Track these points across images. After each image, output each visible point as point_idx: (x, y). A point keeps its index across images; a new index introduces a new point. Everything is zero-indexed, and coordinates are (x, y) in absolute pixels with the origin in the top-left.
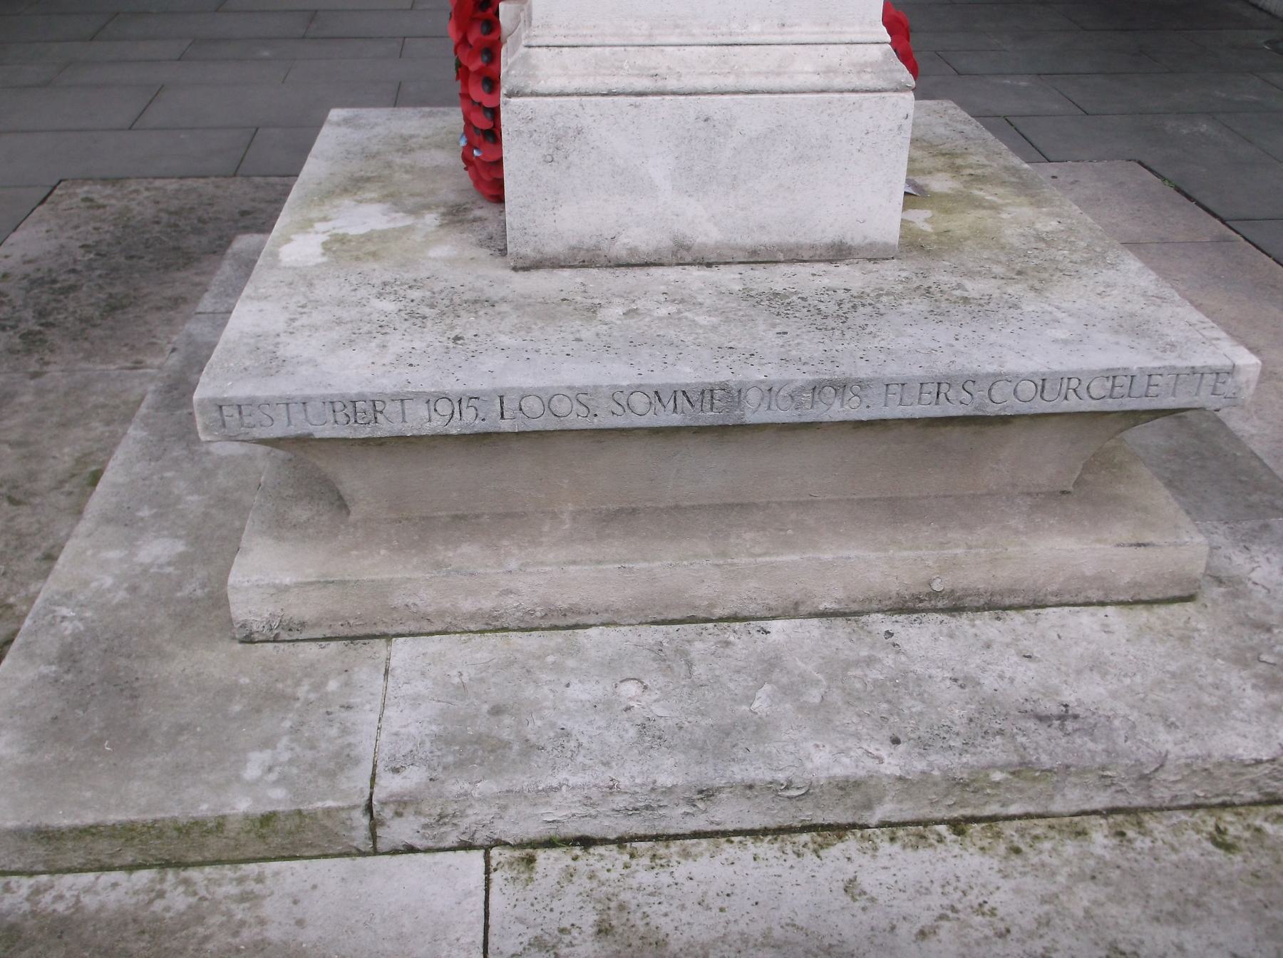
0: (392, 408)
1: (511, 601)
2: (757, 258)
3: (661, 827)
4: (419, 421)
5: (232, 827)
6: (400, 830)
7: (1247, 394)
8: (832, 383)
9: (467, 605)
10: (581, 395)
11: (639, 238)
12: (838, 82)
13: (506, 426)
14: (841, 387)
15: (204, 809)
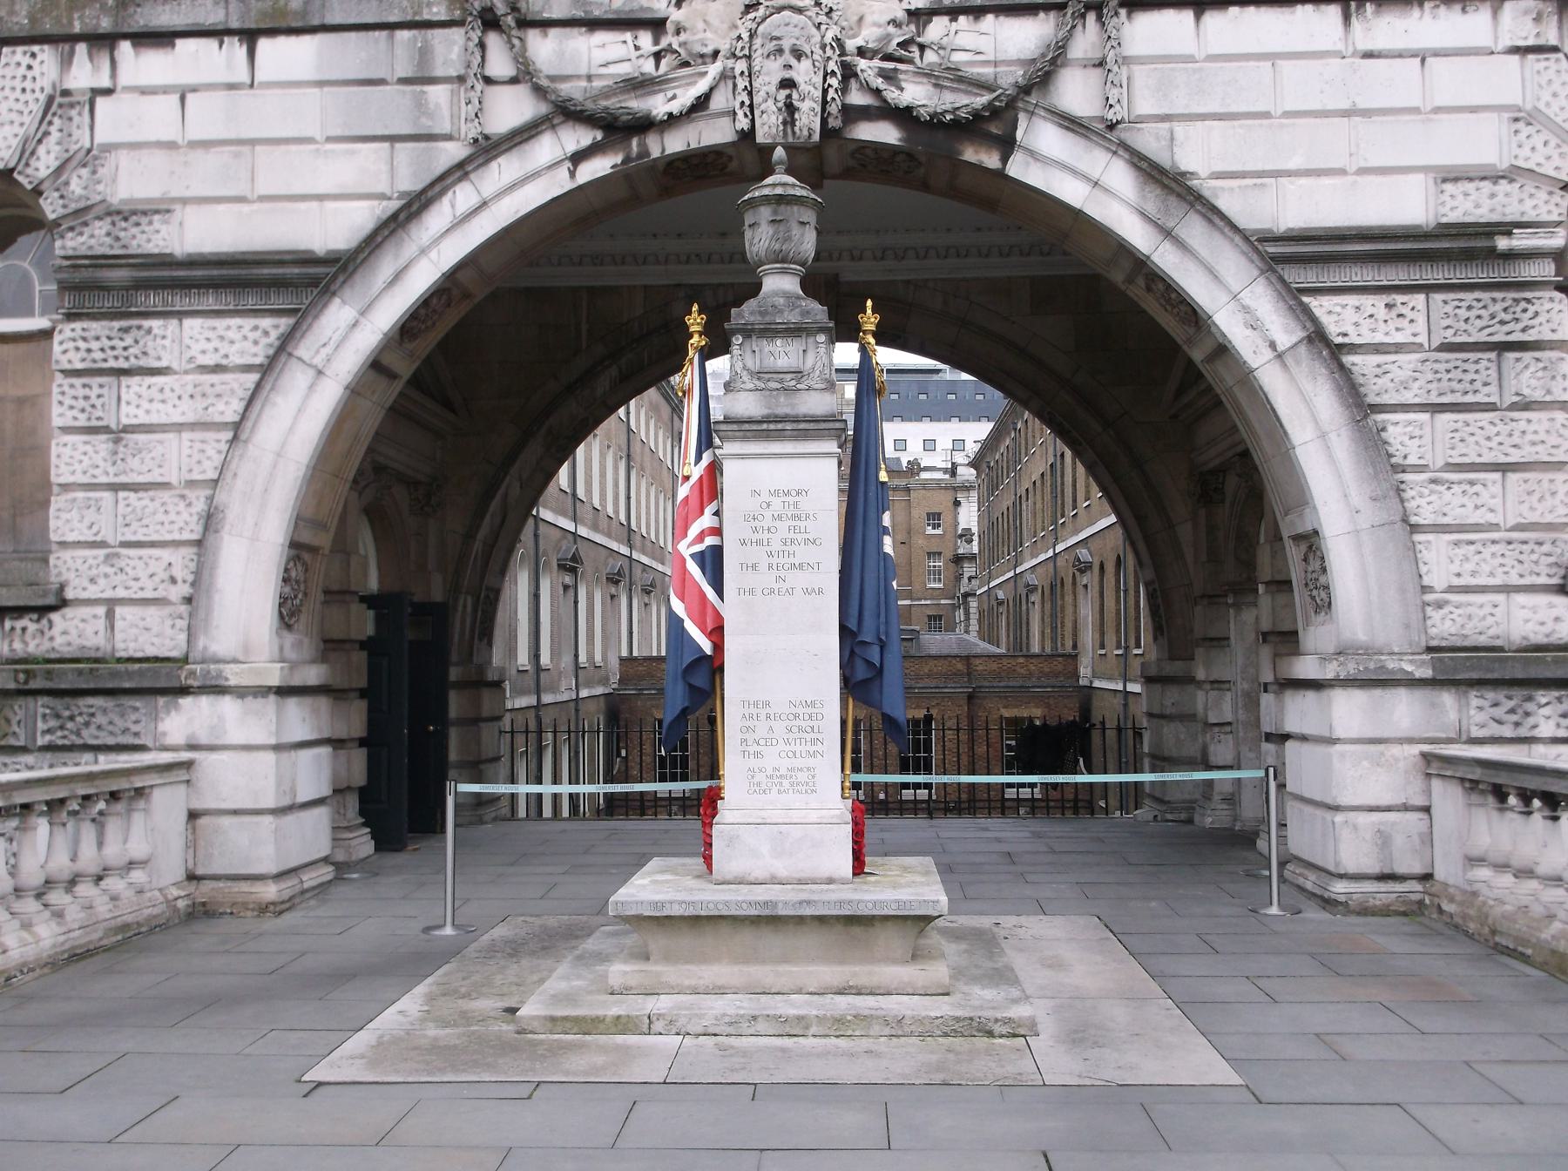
2: (800, 882)
4: (676, 911)
7: (945, 911)
9: (687, 982)
10: (726, 903)
11: (759, 874)
14: (808, 902)
15: (600, 1013)
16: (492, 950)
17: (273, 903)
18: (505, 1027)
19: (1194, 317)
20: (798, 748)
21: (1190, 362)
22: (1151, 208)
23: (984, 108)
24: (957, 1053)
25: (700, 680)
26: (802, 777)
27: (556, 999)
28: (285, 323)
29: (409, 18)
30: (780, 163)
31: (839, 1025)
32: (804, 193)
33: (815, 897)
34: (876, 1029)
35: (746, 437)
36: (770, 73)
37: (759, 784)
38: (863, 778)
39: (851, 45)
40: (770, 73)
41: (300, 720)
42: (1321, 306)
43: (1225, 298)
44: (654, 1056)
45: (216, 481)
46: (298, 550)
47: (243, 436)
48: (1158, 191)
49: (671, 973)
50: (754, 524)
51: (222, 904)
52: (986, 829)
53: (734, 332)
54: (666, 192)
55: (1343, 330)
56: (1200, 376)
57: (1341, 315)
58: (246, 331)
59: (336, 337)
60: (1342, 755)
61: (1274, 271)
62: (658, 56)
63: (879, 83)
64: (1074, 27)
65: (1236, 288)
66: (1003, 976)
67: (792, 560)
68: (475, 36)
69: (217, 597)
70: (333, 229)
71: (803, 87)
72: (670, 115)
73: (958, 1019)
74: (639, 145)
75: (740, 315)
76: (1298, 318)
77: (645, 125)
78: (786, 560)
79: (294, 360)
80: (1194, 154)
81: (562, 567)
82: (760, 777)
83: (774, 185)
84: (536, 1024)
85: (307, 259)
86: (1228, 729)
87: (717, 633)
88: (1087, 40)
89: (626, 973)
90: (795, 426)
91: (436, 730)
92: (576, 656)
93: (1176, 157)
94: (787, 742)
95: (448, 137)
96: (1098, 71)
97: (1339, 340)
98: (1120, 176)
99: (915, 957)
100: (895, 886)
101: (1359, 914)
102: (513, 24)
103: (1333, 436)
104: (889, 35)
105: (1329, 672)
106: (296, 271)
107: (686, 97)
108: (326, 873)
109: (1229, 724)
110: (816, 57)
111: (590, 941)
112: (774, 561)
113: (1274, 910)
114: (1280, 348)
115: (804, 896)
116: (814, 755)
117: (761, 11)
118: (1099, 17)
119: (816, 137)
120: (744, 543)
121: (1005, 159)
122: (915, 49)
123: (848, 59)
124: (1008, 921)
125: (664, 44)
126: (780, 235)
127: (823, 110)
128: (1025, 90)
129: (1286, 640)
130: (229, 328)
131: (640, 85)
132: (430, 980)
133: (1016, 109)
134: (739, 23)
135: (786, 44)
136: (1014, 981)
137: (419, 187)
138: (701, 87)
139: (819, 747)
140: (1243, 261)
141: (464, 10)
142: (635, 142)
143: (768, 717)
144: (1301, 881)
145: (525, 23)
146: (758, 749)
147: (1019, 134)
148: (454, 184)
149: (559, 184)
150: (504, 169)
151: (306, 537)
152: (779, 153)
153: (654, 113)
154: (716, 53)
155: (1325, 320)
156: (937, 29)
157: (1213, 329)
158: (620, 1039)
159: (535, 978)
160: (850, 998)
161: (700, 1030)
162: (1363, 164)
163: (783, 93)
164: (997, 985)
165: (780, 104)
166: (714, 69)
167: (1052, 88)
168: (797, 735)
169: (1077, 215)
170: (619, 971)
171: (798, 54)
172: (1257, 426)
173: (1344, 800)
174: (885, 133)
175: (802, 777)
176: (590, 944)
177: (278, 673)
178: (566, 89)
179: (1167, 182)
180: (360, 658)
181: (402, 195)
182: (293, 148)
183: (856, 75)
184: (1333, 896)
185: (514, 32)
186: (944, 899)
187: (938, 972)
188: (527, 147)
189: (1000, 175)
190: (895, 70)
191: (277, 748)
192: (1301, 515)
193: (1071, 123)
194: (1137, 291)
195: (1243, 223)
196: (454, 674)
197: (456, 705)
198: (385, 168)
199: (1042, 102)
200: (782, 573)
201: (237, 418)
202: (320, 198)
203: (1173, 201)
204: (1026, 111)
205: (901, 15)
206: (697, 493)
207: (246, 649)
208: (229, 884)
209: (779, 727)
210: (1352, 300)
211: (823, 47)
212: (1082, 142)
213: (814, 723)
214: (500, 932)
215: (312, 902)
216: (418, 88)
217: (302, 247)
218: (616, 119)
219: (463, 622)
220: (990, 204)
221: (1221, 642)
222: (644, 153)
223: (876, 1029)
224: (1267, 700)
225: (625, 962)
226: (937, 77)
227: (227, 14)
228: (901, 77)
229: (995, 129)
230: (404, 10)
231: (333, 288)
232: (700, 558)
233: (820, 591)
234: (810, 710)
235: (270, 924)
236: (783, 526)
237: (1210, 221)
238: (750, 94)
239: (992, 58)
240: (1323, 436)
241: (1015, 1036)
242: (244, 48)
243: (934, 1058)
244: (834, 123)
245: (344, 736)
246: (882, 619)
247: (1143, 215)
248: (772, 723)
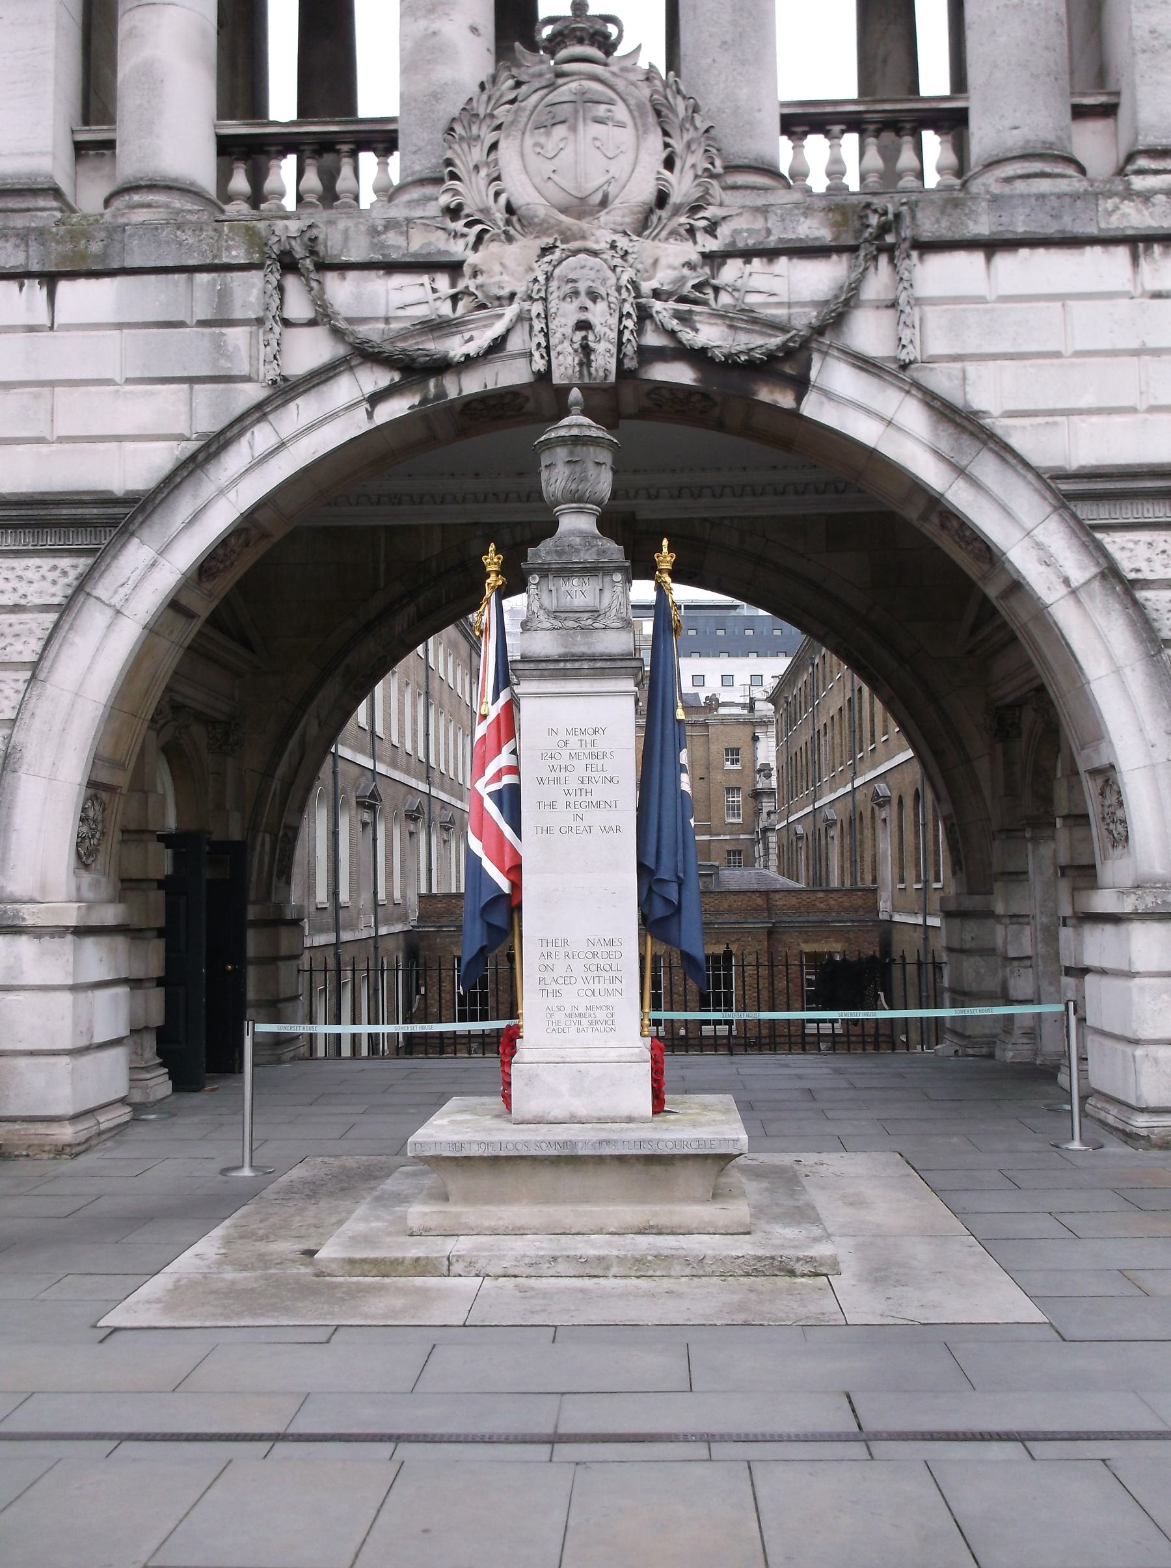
0: (467, 1146)
1: (501, 1223)
2: (600, 1121)
3: (540, 1273)
4: (475, 1151)
5: (407, 1262)
6: (457, 1268)
7: (746, 1149)
8: (604, 1141)
9: (486, 1224)
10: (526, 1144)
11: (557, 1112)
12: (624, 1059)
13: (502, 1154)
14: (608, 1142)
15: (399, 1254)
16: (290, 1191)
17: (69, 1145)
18: (303, 1270)
19: (988, 554)
20: (596, 986)
21: (985, 599)
22: (944, 446)
23: (779, 348)
24: (761, 1293)
25: (498, 919)
26: (601, 1015)
27: (355, 1241)
28: (84, 563)
29: (208, 261)
30: (577, 404)
31: (640, 1265)
32: (600, 434)
33: (615, 1137)
34: (677, 1269)
35: (543, 675)
36: (566, 315)
38: (663, 1015)
39: (646, 287)
40: (566, 315)
41: (97, 962)
42: (1113, 542)
43: (1019, 535)
44: (453, 1298)
45: (14, 721)
46: (95, 789)
47: (42, 676)
48: (951, 430)
49: (470, 1214)
50: (551, 762)
51: (17, 1147)
52: (787, 1066)
53: (531, 571)
54: (462, 432)
55: (1136, 566)
56: (994, 612)
57: (1133, 552)
58: (43, 571)
59: (135, 577)
60: (1142, 989)
61: (1067, 508)
62: (455, 299)
63: (674, 324)
64: (866, 269)
65: (1029, 525)
66: (804, 1214)
67: (589, 798)
68: (274, 279)
69: (14, 837)
70: (131, 470)
71: (599, 329)
72: (467, 356)
73: (759, 1259)
74: (436, 386)
75: (536, 555)
76: (1091, 554)
77: (442, 366)
78: (584, 798)
79: (92, 600)
80: (988, 393)
81: (361, 804)
83: (570, 426)
84: (334, 1266)
85: (105, 499)
86: (1028, 963)
87: (515, 871)
88: (879, 281)
89: (425, 1214)
90: (591, 664)
91: (234, 969)
92: (375, 893)
93: (969, 397)
95: (247, 379)
96: (891, 312)
97: (1132, 576)
98: (913, 415)
99: (716, 1195)
100: (695, 1124)
101: (1160, 1148)
102: (311, 268)
103: (1127, 671)
104: (683, 277)
105: (1128, 905)
106: (95, 511)
107: (483, 338)
108: (122, 1114)
109: (1029, 958)
110: (612, 299)
111: (389, 1181)
112: (572, 799)
113: (1076, 1145)
114: (1074, 584)
115: (603, 1136)
116: (613, 993)
117: (557, 254)
118: (891, 260)
119: (612, 378)
120: (541, 781)
121: (799, 399)
122: (709, 291)
123: (643, 300)
124: (809, 1158)
125: (461, 286)
126: (576, 475)
127: (619, 351)
128: (819, 331)
129: (1084, 874)
130: (27, 568)
131: (437, 327)
132: (227, 1222)
133: (810, 350)
134: (536, 265)
135: (582, 287)
136: (817, 1220)
137: (217, 428)
138: (498, 328)
140: (1036, 498)
141: (263, 253)
142: (432, 383)
143: (567, 956)
144: (1102, 1115)
145: (324, 266)
146: (557, 987)
147: (813, 374)
148: (253, 424)
149: (357, 425)
150: (302, 411)
151: (104, 777)
152: (575, 394)
153: (451, 354)
154: (512, 296)
155: (1118, 556)
156: (731, 271)
157: (1007, 566)
158: (419, 1281)
159: (334, 1220)
160: (650, 1239)
161: (500, 1271)
162: (1153, 402)
163: (579, 335)
164: (799, 1223)
165: (576, 346)
166: (511, 312)
167: (845, 329)
168: (596, 974)
169: (871, 454)
170: (418, 1213)
171: (594, 296)
172: (1050, 658)
173: (1146, 1033)
174: (681, 374)
175: (601, 1015)
176: (389, 1185)
177: (74, 913)
178: (364, 331)
179: (959, 421)
180: (158, 897)
181: (201, 435)
182: (93, 389)
183: (651, 317)
184: (1135, 1130)
185: (312, 276)
186: (744, 1137)
187: (739, 1211)
188: (324, 388)
189: (795, 414)
190: (690, 312)
191: (74, 988)
192: (1097, 750)
193: (865, 364)
194: (931, 529)
195: (1036, 460)
196: (252, 912)
197: (254, 943)
198: (183, 408)
199: (839, 344)
200: (580, 812)
201: (35, 658)
202: (119, 439)
203: (966, 440)
204: (819, 351)
205: (695, 257)
206: (494, 732)
207: (43, 888)
208: (25, 1125)
209: (578, 965)
210: (1144, 536)
211: (619, 289)
212: (874, 382)
213: (614, 962)
214: (298, 1173)
215: (109, 1144)
216: (217, 330)
217: (102, 488)
218: (413, 360)
219: (261, 861)
220: (785, 443)
221: (1019, 876)
222: (441, 393)
223: (677, 1269)
224: (1066, 933)
225: (425, 1203)
226: (732, 319)
227: (27, 258)
228: (696, 318)
229: (789, 369)
230: (203, 254)
231: (132, 528)
232: (497, 797)
233: (618, 829)
234: (608, 949)
235: (66, 1166)
236: (580, 765)
237: (1003, 459)
238: (546, 335)
239: (786, 300)
240: (1118, 671)
241: (817, 1275)
242: (45, 290)
243: (736, 1298)
244: (629, 364)
245: (141, 975)
246: (680, 857)
247: (936, 453)
248: (571, 962)
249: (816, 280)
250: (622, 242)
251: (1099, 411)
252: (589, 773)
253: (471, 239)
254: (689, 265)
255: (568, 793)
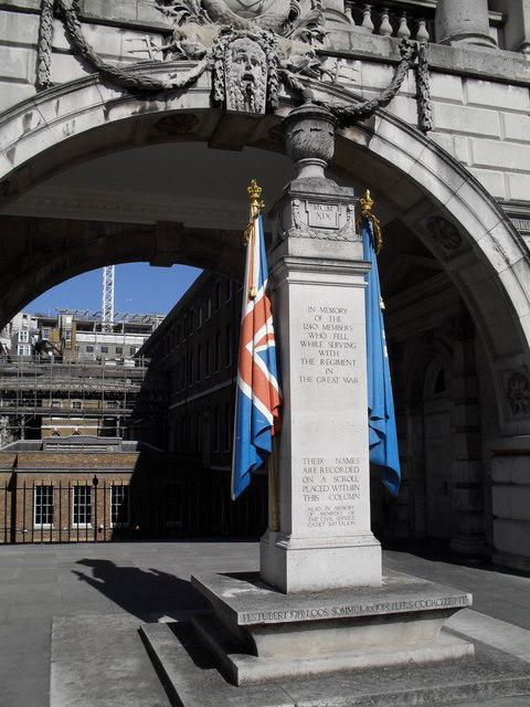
26: (345, 513)
37: (316, 519)
39: (284, 63)
54: (150, 140)
67: (336, 358)
72: (174, 85)
80: (462, 151)
82: (317, 514)
94: (335, 488)
98: (429, 158)
107: (182, 77)
112: (325, 358)
119: (263, 111)
121: (368, 141)
138: (194, 72)
139: (357, 492)
147: (376, 127)
149: (96, 120)
154: (201, 56)
156: (329, 63)
163: (246, 82)
171: (255, 62)
175: (345, 513)
189: (365, 149)
204: (380, 116)
211: (268, 61)
233: (356, 381)
236: (330, 333)
249: (378, 76)
250: (269, 35)
251: (518, 171)
252: (336, 340)
253: (179, 18)
254: (310, 54)
255: (322, 353)
